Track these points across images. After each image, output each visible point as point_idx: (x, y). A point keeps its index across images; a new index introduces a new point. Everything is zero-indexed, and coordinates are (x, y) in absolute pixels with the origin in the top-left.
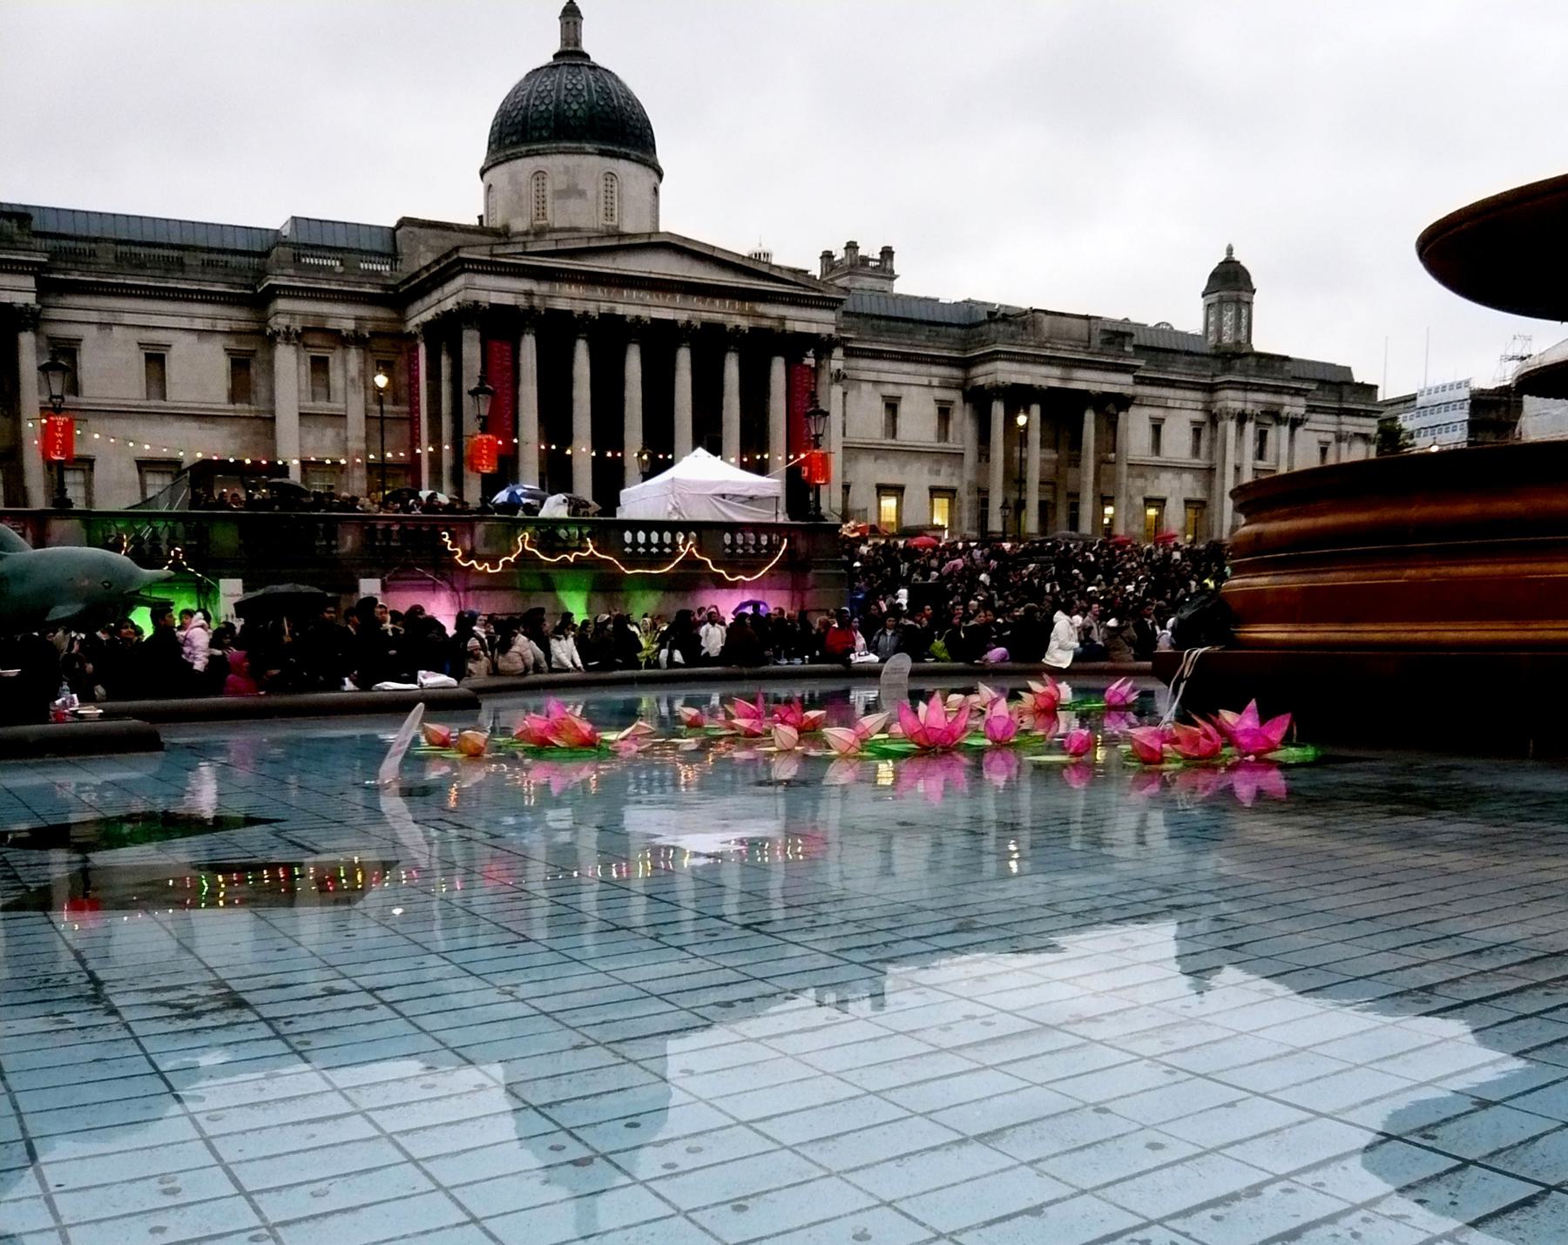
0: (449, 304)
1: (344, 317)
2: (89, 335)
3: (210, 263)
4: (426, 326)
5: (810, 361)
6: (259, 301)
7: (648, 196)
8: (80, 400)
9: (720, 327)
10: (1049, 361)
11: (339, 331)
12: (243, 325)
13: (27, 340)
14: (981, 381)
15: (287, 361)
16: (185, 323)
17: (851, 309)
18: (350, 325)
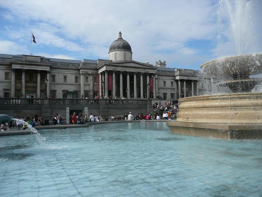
0: (104, 70)
1: (90, 72)
3: (73, 65)
4: (101, 73)
5: (152, 77)
6: (79, 70)
7: (130, 56)
9: (140, 72)
10: (186, 76)
11: (89, 74)
12: (77, 73)
13: (48, 75)
14: (177, 79)
15: (82, 78)
17: (158, 70)
18: (91, 73)
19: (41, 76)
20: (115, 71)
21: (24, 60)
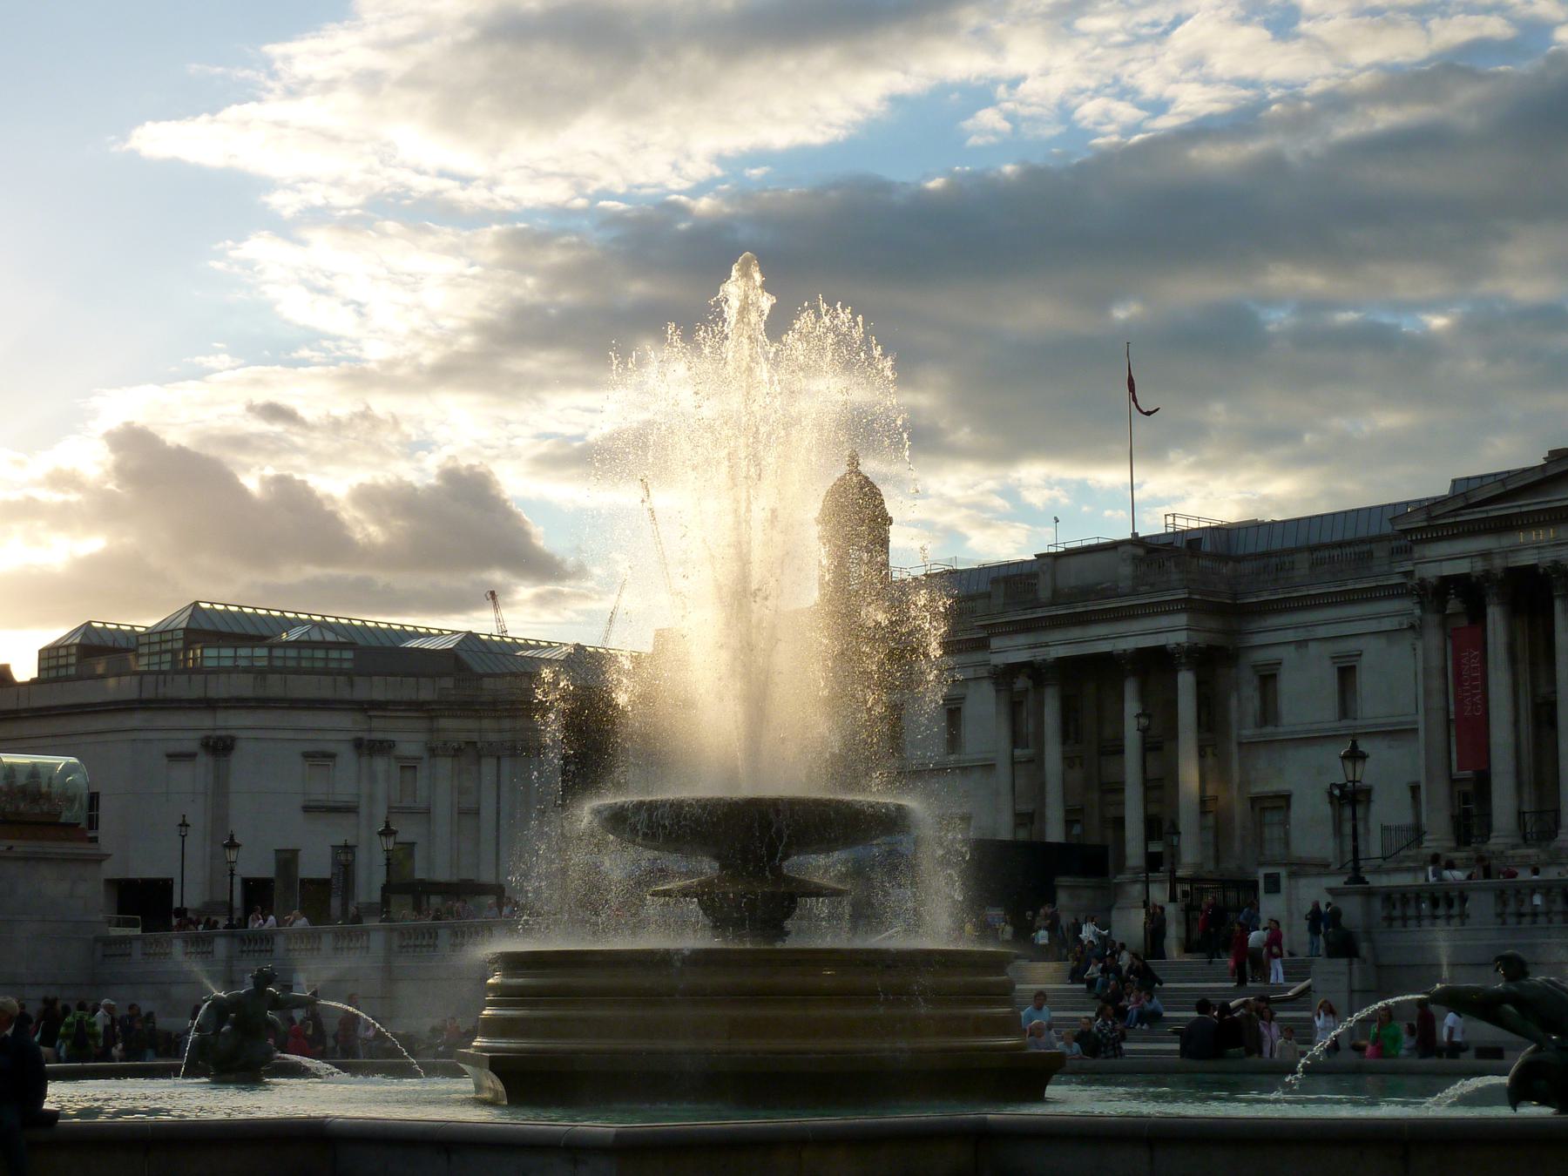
2: (1287, 654)
8: (1281, 729)
13: (1186, 681)
16: (1373, 626)
19: (1143, 697)
20: (1487, 575)
21: (1044, 594)
